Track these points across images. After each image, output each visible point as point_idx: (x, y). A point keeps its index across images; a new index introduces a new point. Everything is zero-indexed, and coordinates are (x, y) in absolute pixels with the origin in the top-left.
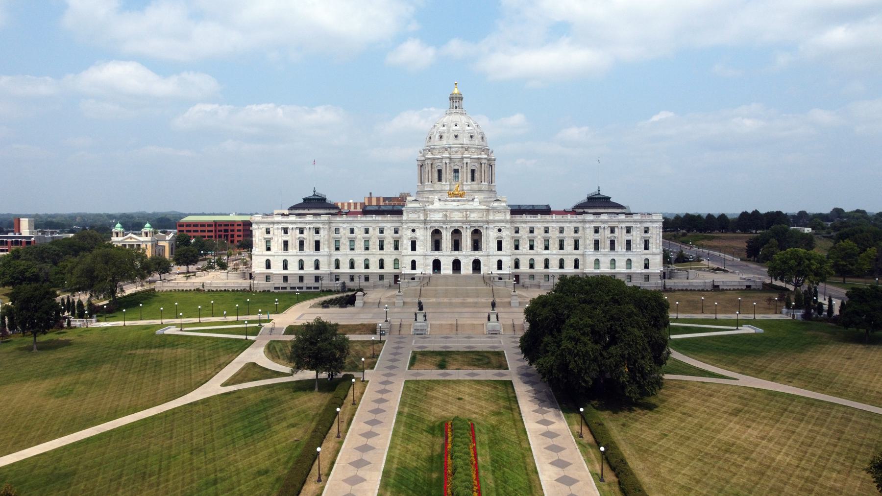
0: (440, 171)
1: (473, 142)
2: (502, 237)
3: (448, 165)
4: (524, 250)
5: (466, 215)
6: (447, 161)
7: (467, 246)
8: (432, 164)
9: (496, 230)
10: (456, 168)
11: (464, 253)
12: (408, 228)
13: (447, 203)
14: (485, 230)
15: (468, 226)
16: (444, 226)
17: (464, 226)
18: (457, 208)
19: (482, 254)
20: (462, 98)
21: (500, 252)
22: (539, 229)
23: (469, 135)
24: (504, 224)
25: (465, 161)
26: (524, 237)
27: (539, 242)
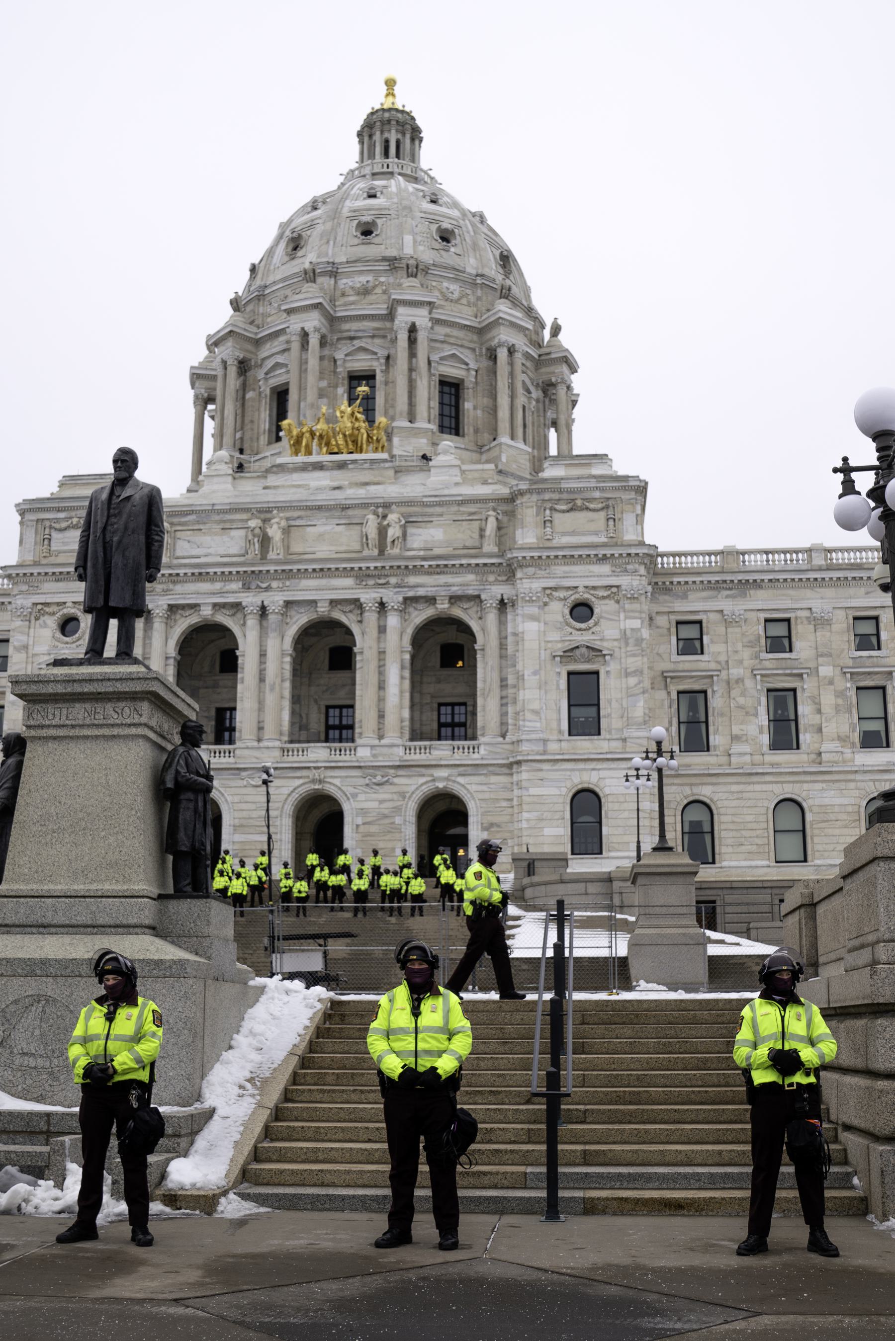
0: (281, 396)
1: (449, 257)
2: (596, 652)
3: (314, 341)
4: (736, 748)
5: (382, 532)
6: (312, 322)
7: (381, 716)
8: (243, 367)
9: (559, 610)
10: (361, 363)
11: (363, 753)
12: (40, 610)
13: (272, 480)
14: (492, 617)
15: (393, 598)
16: (250, 600)
17: (368, 596)
18: (324, 498)
19: (474, 758)
20: (416, 134)
21: (584, 745)
22: (820, 622)
23: (434, 227)
24: (606, 569)
25: (404, 315)
26: (736, 672)
27: (828, 700)
